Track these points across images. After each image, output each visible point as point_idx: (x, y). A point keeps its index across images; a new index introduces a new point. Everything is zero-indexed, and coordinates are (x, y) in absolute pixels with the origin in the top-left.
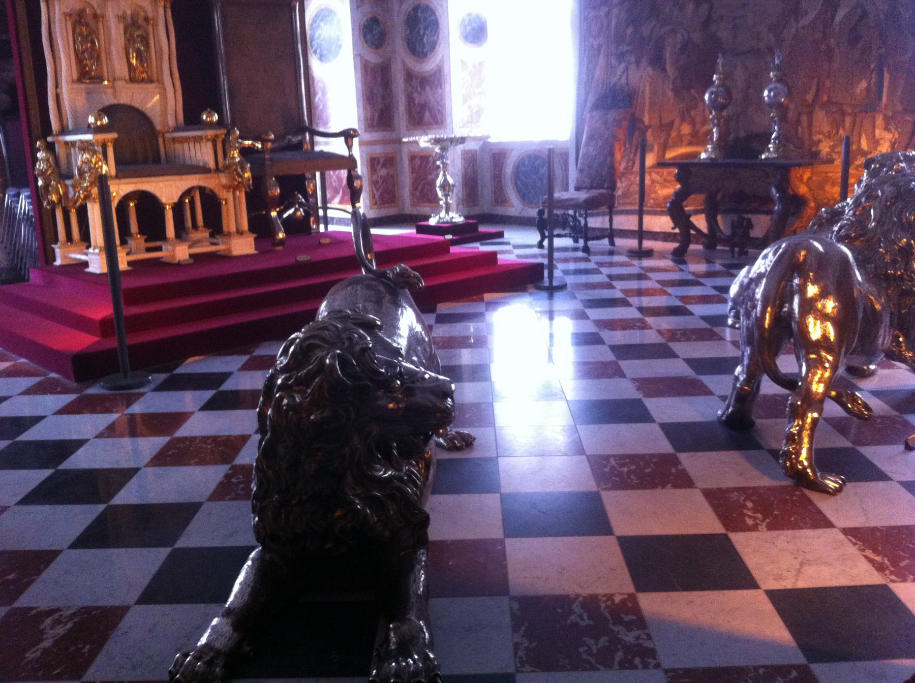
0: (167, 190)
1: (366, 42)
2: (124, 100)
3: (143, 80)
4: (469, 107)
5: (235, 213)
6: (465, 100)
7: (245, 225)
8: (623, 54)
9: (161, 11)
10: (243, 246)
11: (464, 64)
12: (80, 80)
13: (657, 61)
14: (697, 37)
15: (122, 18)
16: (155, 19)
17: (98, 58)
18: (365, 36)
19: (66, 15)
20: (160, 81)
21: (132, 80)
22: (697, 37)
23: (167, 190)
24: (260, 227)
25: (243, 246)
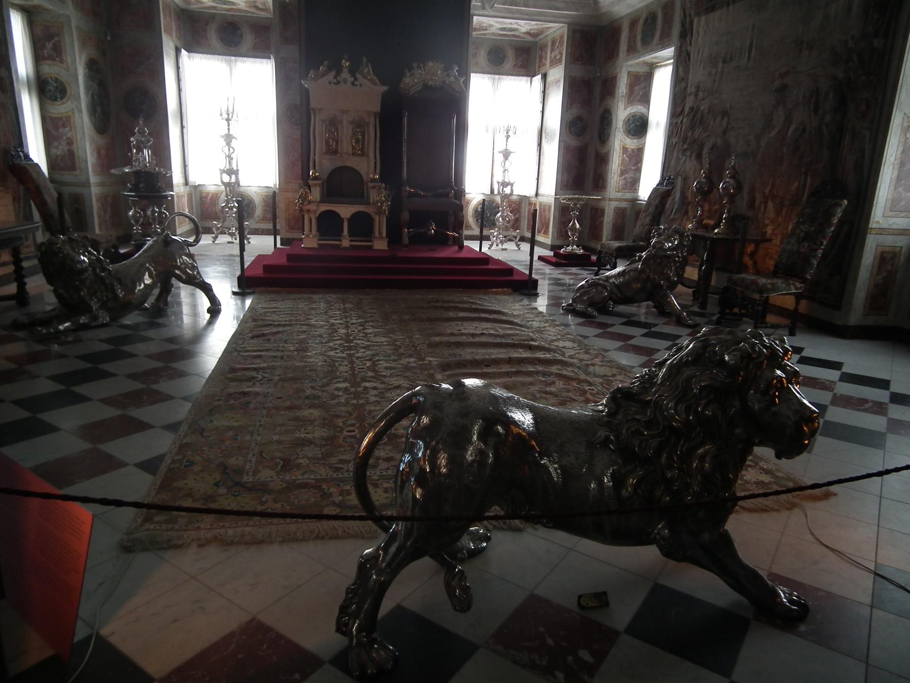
0: (345, 211)
1: (571, 132)
2: (349, 164)
3: (359, 155)
4: (625, 179)
5: (381, 226)
6: (622, 173)
7: (384, 234)
8: (685, 150)
9: (372, 119)
10: (380, 245)
11: (625, 149)
12: (325, 154)
13: (699, 157)
14: (719, 141)
15: (352, 123)
16: (368, 124)
17: (337, 143)
18: (570, 129)
19: (324, 121)
20: (368, 156)
21: (354, 154)
22: (719, 141)
23: (345, 211)
24: (394, 237)
25: (380, 245)
